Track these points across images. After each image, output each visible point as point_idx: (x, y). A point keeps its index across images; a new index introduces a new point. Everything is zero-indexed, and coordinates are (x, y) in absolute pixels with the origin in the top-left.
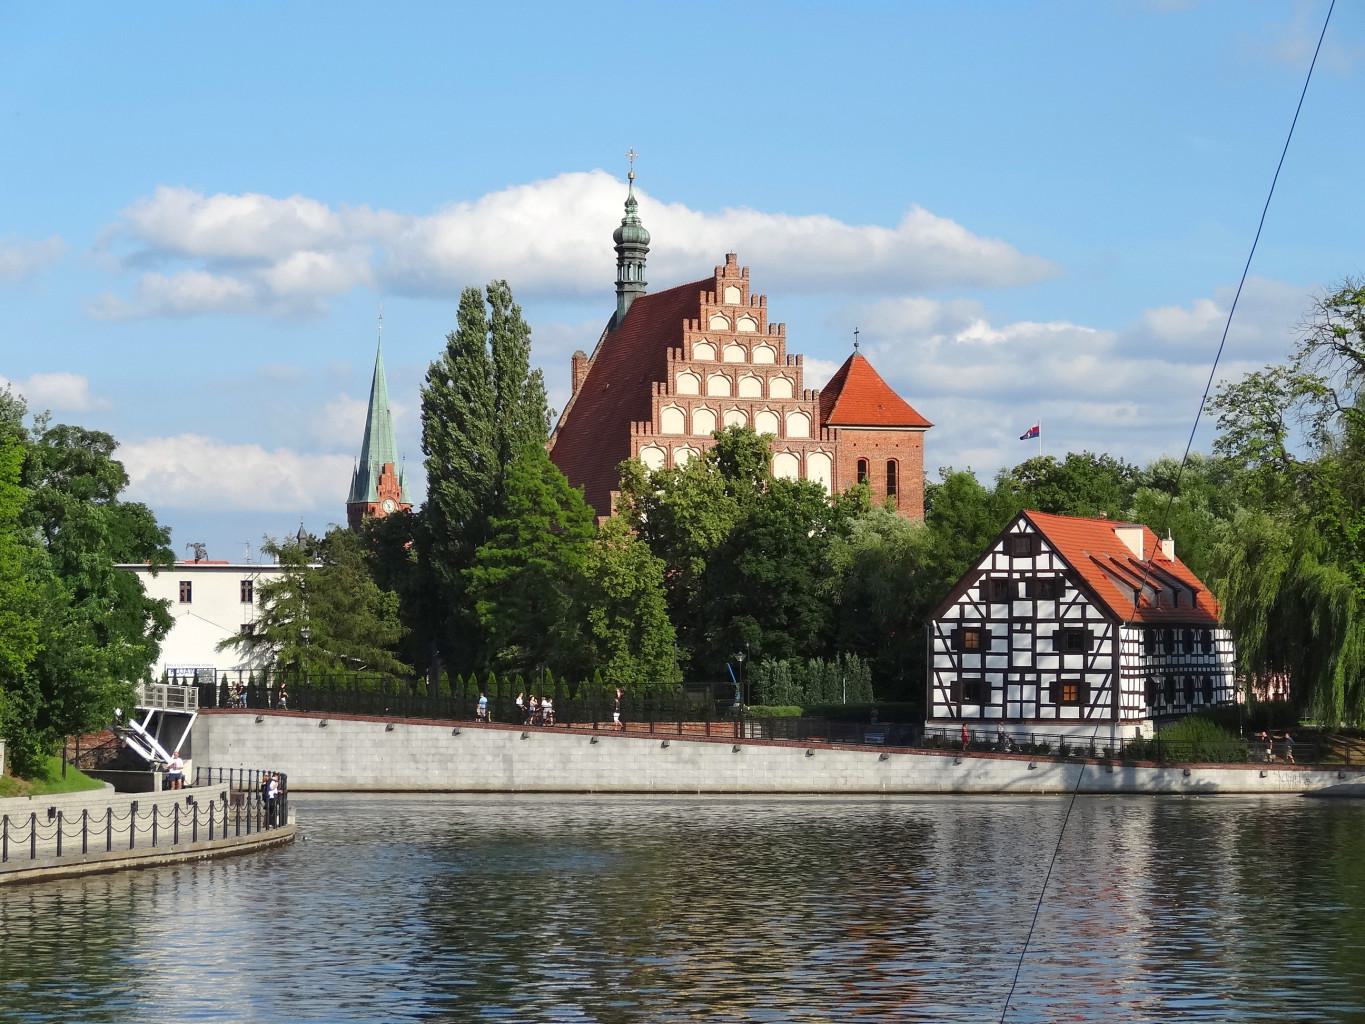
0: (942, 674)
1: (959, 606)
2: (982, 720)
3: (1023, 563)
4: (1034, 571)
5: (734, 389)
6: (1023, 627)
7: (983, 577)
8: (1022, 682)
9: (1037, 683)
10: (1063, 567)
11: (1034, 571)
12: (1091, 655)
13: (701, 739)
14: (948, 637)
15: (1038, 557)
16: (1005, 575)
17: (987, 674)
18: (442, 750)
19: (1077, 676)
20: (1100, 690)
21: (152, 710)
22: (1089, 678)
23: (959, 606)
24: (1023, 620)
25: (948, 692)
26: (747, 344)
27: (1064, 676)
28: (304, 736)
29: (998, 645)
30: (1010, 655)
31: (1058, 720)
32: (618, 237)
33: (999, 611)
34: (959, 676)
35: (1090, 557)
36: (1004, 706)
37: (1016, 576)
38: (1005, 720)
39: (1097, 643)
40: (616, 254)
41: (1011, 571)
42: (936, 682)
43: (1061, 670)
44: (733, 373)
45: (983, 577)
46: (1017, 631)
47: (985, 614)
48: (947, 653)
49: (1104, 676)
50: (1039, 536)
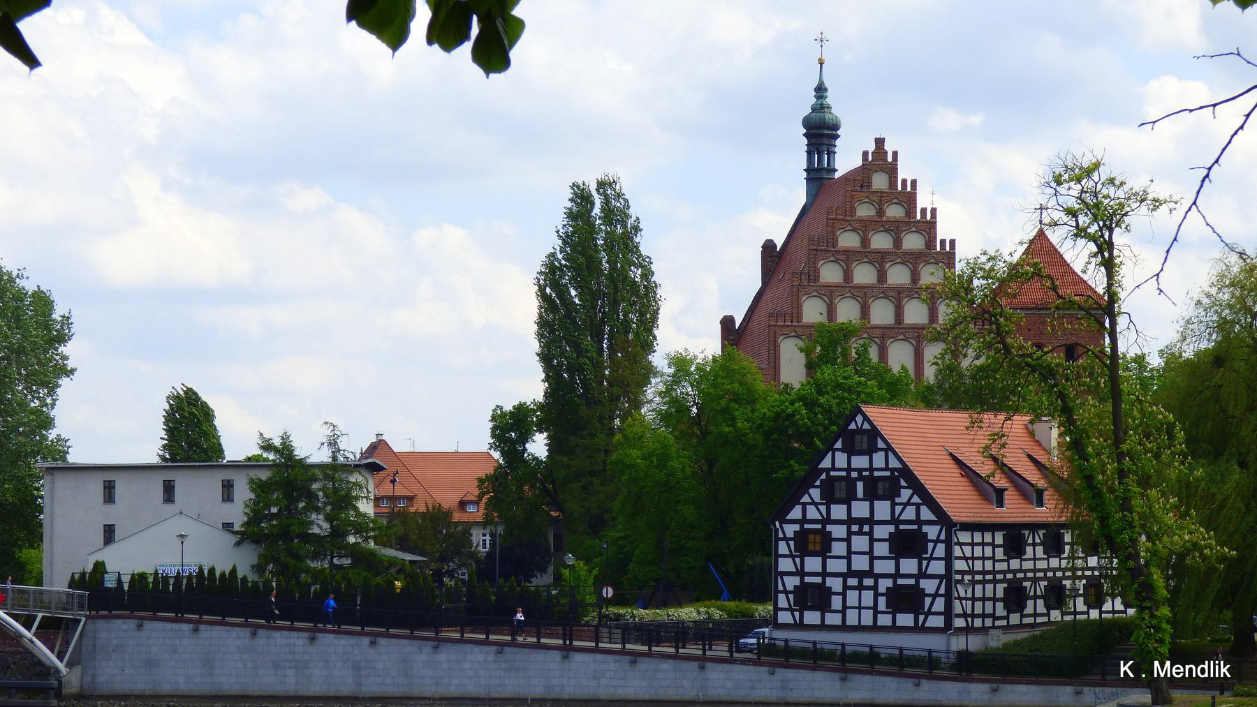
2: (822, 627)
3: (860, 462)
4: (871, 469)
5: (882, 276)
6: (861, 528)
8: (860, 588)
9: (875, 588)
10: (899, 466)
11: (871, 469)
12: (926, 559)
13: (531, 646)
14: (791, 539)
16: (844, 474)
17: (828, 579)
18: (297, 656)
19: (912, 582)
20: (935, 596)
21: (40, 615)
22: (924, 583)
24: (861, 522)
25: (791, 596)
26: (896, 229)
28: (177, 642)
29: (839, 548)
30: (848, 558)
31: (894, 628)
32: (807, 122)
33: (839, 511)
34: (802, 580)
35: (951, 455)
37: (854, 475)
38: (844, 627)
39: (931, 545)
40: (805, 141)
41: (849, 469)
42: (780, 587)
43: (897, 575)
44: (880, 260)
45: (824, 476)
48: (791, 556)
49: (937, 581)
50: (874, 433)
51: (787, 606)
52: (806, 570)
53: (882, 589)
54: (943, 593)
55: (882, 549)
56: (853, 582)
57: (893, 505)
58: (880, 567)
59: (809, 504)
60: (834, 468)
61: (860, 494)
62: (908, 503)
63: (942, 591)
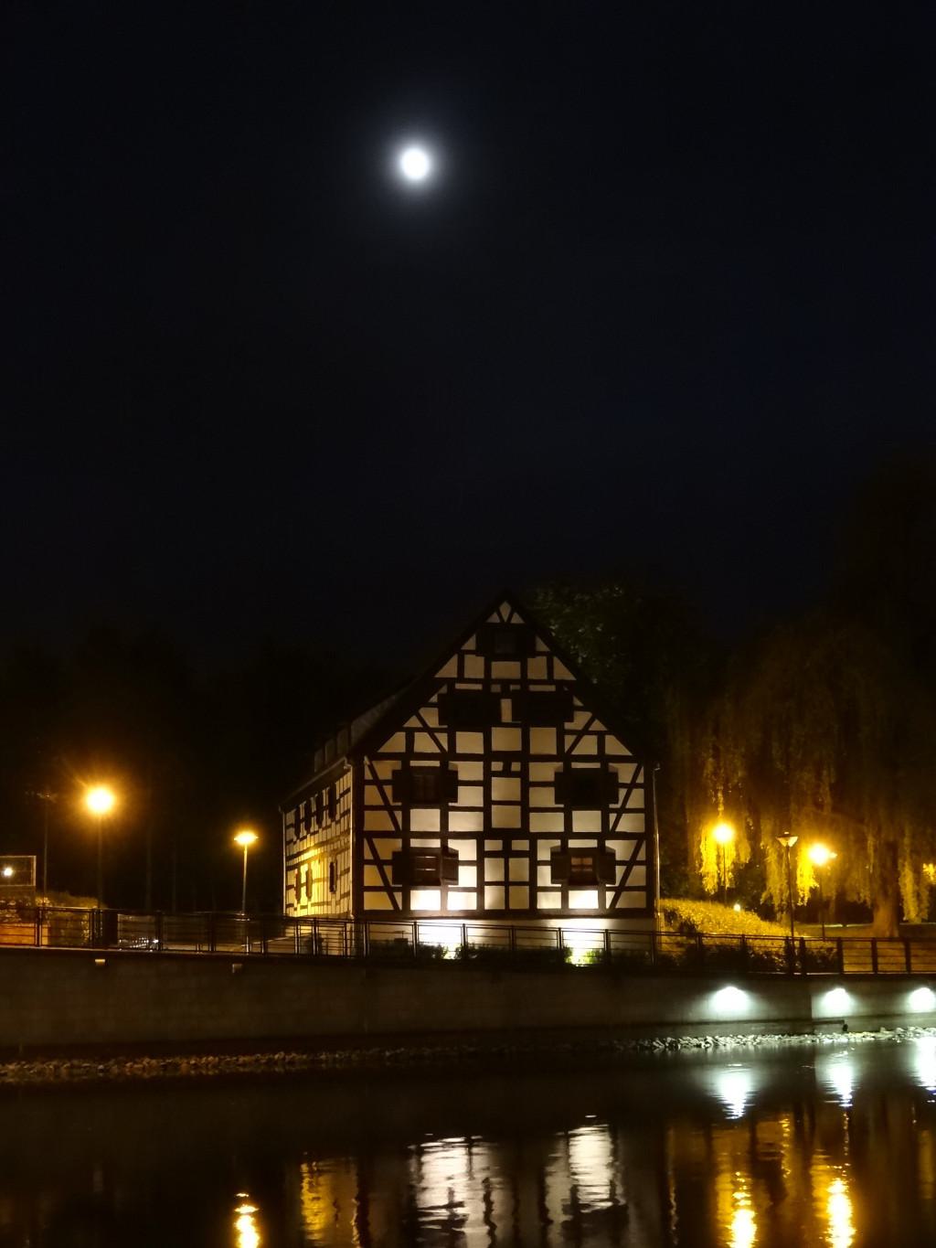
0: (375, 841)
1: (403, 734)
3: (506, 669)
4: (524, 680)
7: (444, 690)
9: (531, 855)
11: (524, 680)
14: (387, 782)
15: (531, 661)
16: (479, 687)
19: (593, 843)
22: (609, 844)
23: (403, 734)
24: (507, 757)
25: (388, 870)
27: (573, 844)
31: (564, 913)
33: (469, 742)
36: (480, 890)
37: (496, 688)
39: (622, 793)
41: (487, 681)
42: (368, 855)
43: (568, 833)
45: (444, 690)
47: (446, 746)
48: (386, 807)
49: (634, 842)
51: (380, 883)
52: (414, 828)
53: (544, 854)
54: (644, 859)
55: (543, 797)
56: (490, 845)
57: (561, 735)
58: (538, 823)
59: (419, 730)
60: (461, 679)
61: (507, 715)
62: (586, 731)
63: (642, 856)
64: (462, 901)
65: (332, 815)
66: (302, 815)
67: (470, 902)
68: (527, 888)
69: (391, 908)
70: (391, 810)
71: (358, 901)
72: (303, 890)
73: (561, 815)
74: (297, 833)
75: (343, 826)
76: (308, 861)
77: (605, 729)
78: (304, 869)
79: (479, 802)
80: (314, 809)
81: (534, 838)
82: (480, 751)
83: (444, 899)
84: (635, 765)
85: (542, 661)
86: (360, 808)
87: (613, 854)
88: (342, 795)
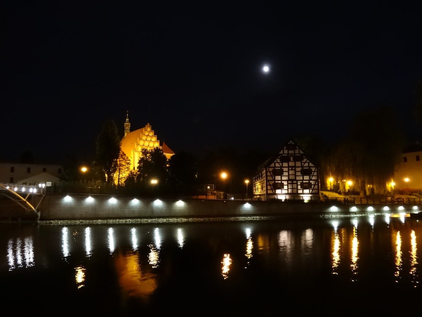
0: (270, 182)
3: (291, 152)
4: (295, 154)
7: (281, 156)
9: (297, 183)
11: (295, 154)
16: (287, 155)
19: (308, 182)
22: (311, 181)
24: (292, 167)
25: (272, 186)
27: (304, 182)
29: (286, 174)
31: (303, 194)
33: (285, 164)
36: (288, 190)
37: (290, 155)
41: (288, 154)
42: (268, 184)
43: (303, 180)
45: (281, 156)
46: (290, 170)
47: (281, 165)
51: (270, 189)
52: (276, 179)
53: (299, 183)
55: (299, 174)
56: (289, 182)
58: (298, 178)
59: (276, 163)
61: (292, 160)
62: (306, 162)
63: (317, 184)
64: (285, 191)
65: (262, 177)
66: (256, 177)
67: (286, 192)
68: (296, 189)
69: (272, 193)
70: (272, 176)
71: (267, 192)
72: (257, 190)
73: (302, 177)
74: (255, 180)
75: (264, 179)
76: (257, 185)
77: (309, 162)
78: (257, 187)
79: (287, 175)
80: (258, 176)
81: (297, 181)
82: (287, 166)
83: (282, 191)
84: (315, 168)
85: (298, 150)
86: (267, 176)
87: (311, 183)
88: (263, 174)
